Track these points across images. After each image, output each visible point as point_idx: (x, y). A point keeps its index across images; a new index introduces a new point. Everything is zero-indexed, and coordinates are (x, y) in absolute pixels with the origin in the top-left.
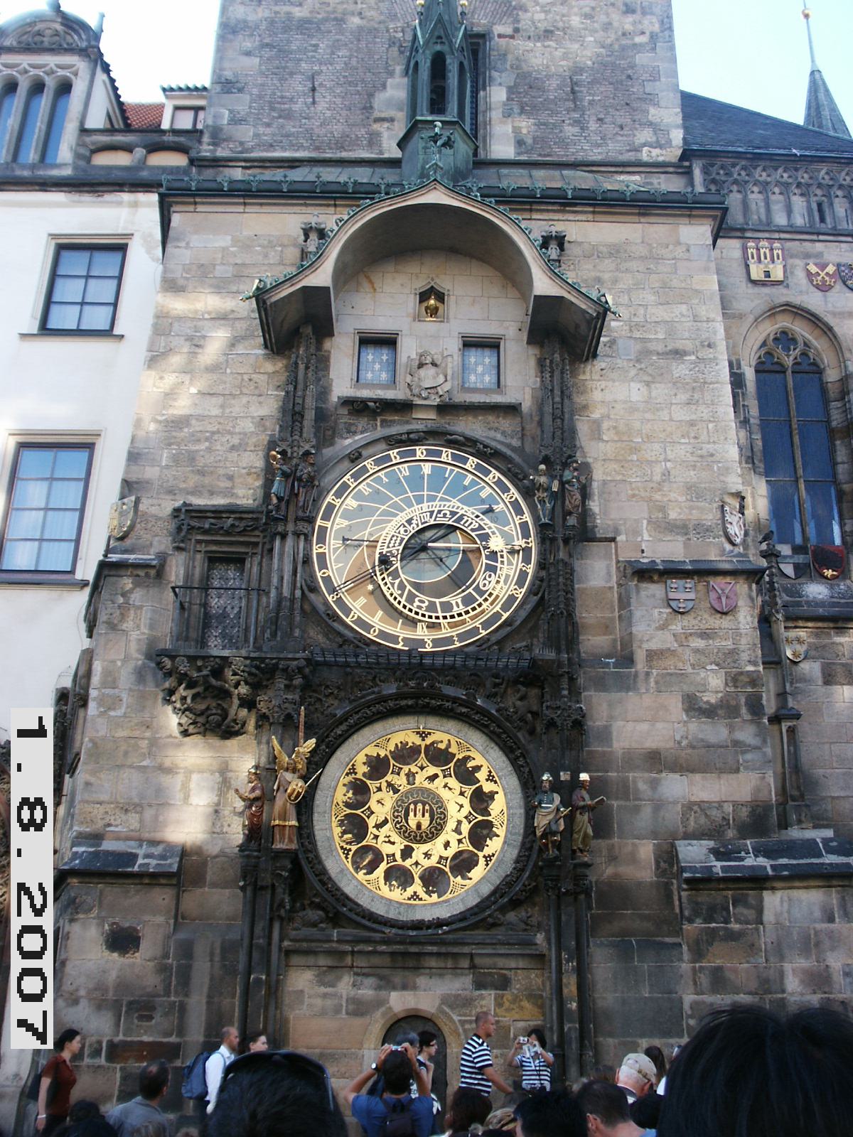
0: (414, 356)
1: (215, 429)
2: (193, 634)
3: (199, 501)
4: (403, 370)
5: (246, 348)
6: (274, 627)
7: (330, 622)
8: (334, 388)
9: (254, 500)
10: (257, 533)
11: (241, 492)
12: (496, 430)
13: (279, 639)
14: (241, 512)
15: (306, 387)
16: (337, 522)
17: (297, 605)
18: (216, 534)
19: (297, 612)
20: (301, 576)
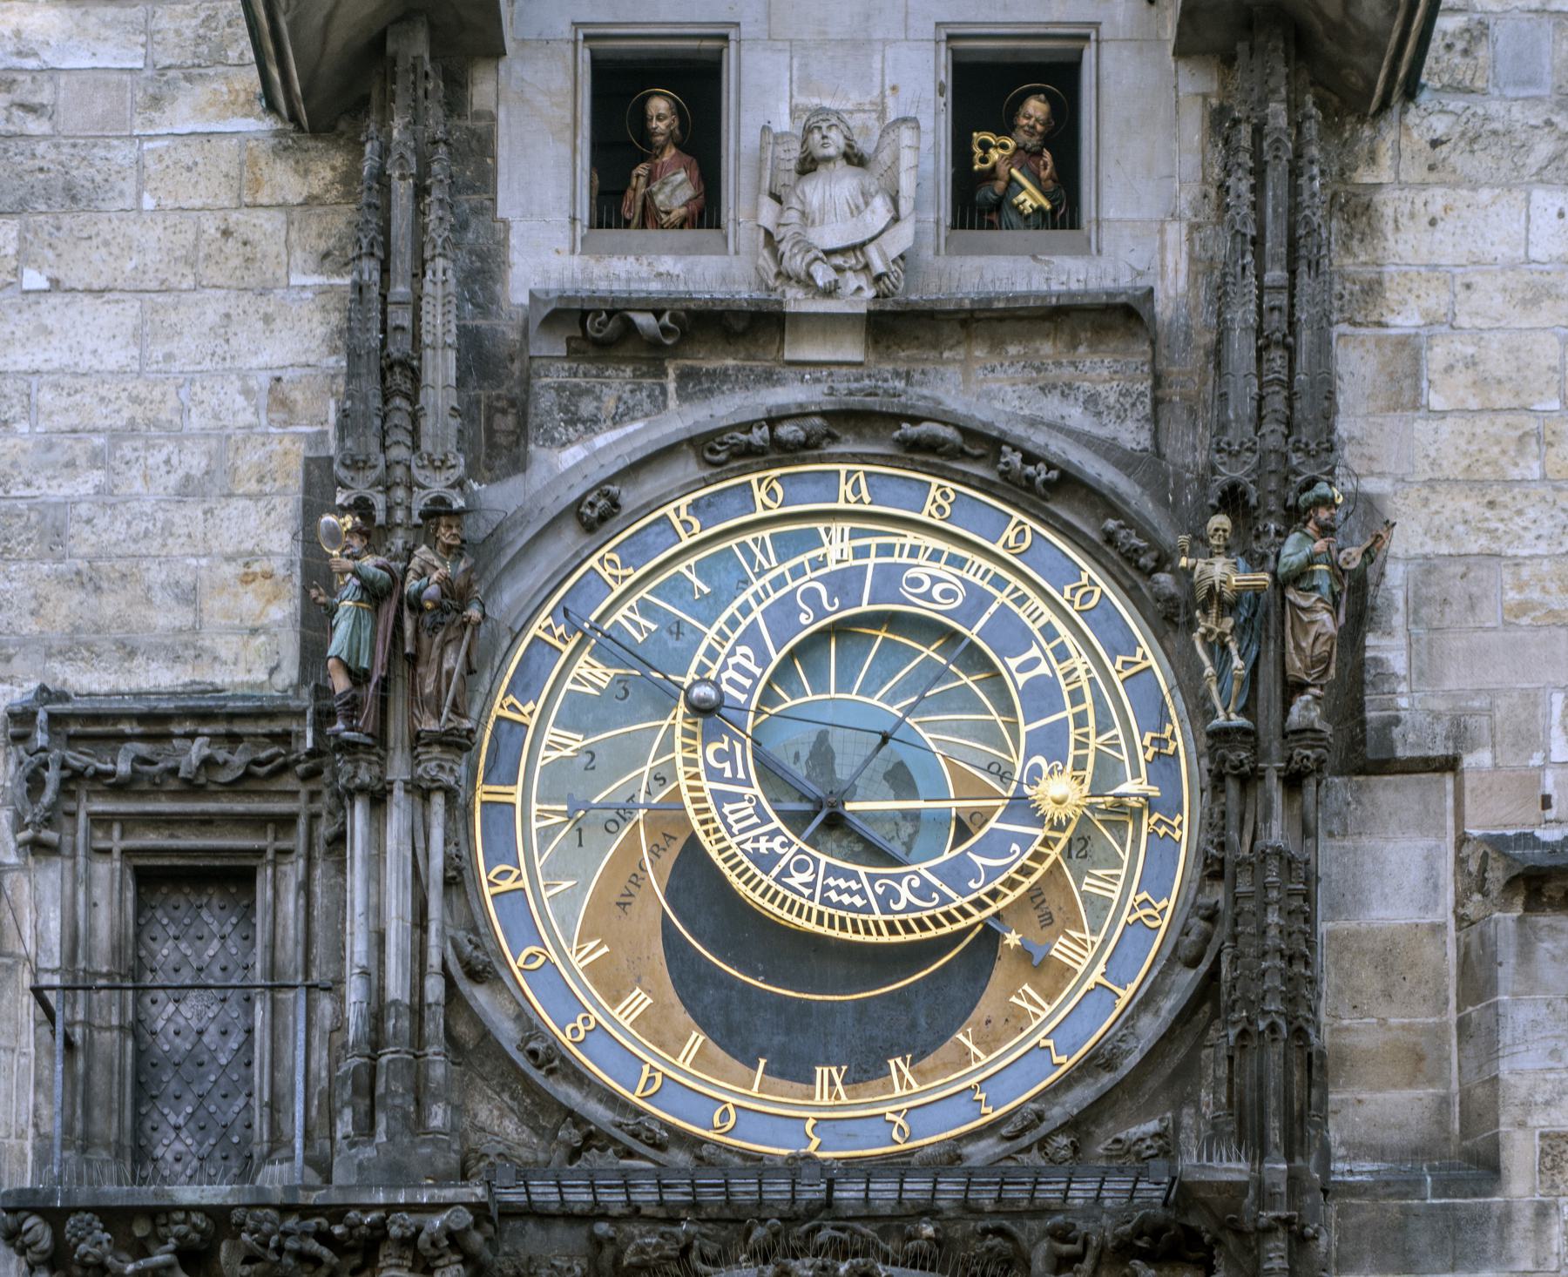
0: (783, 122)
1: (119, 422)
2: (108, 1126)
3: (92, 681)
4: (746, 178)
5: (200, 111)
6: (363, 1104)
7: (538, 1076)
8: (514, 257)
9: (272, 671)
10: (289, 782)
11: (226, 647)
12: (1067, 390)
13: (381, 1137)
14: (232, 717)
15: (419, 274)
16: (545, 742)
17: (434, 1026)
18: (156, 791)
19: (435, 1051)
20: (442, 933)
